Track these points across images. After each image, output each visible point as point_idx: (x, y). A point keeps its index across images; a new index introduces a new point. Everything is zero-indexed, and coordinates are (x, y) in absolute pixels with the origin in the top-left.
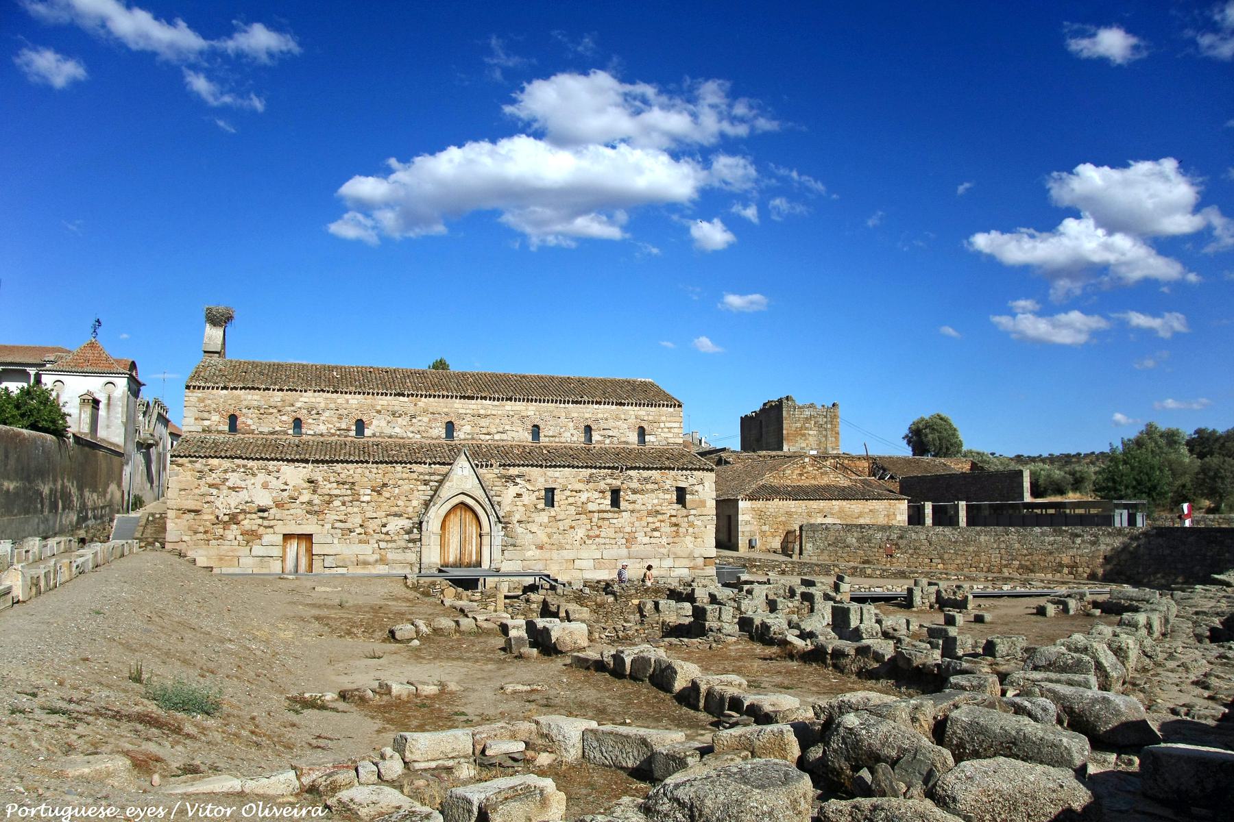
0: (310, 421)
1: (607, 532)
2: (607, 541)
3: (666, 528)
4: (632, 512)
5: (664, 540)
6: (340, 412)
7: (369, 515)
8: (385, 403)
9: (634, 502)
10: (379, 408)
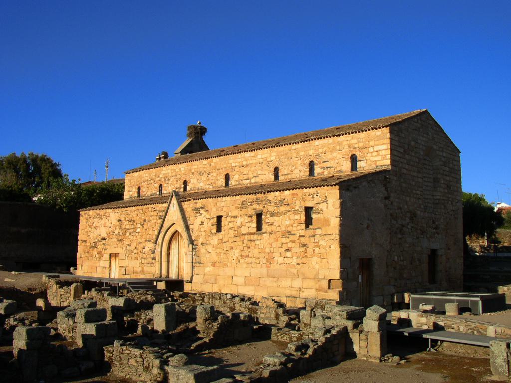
0: (165, 185)
1: (255, 252)
2: (253, 260)
3: (297, 249)
4: (271, 233)
5: (295, 261)
6: (177, 177)
7: (139, 241)
8: (196, 167)
9: (272, 224)
10: (193, 171)
